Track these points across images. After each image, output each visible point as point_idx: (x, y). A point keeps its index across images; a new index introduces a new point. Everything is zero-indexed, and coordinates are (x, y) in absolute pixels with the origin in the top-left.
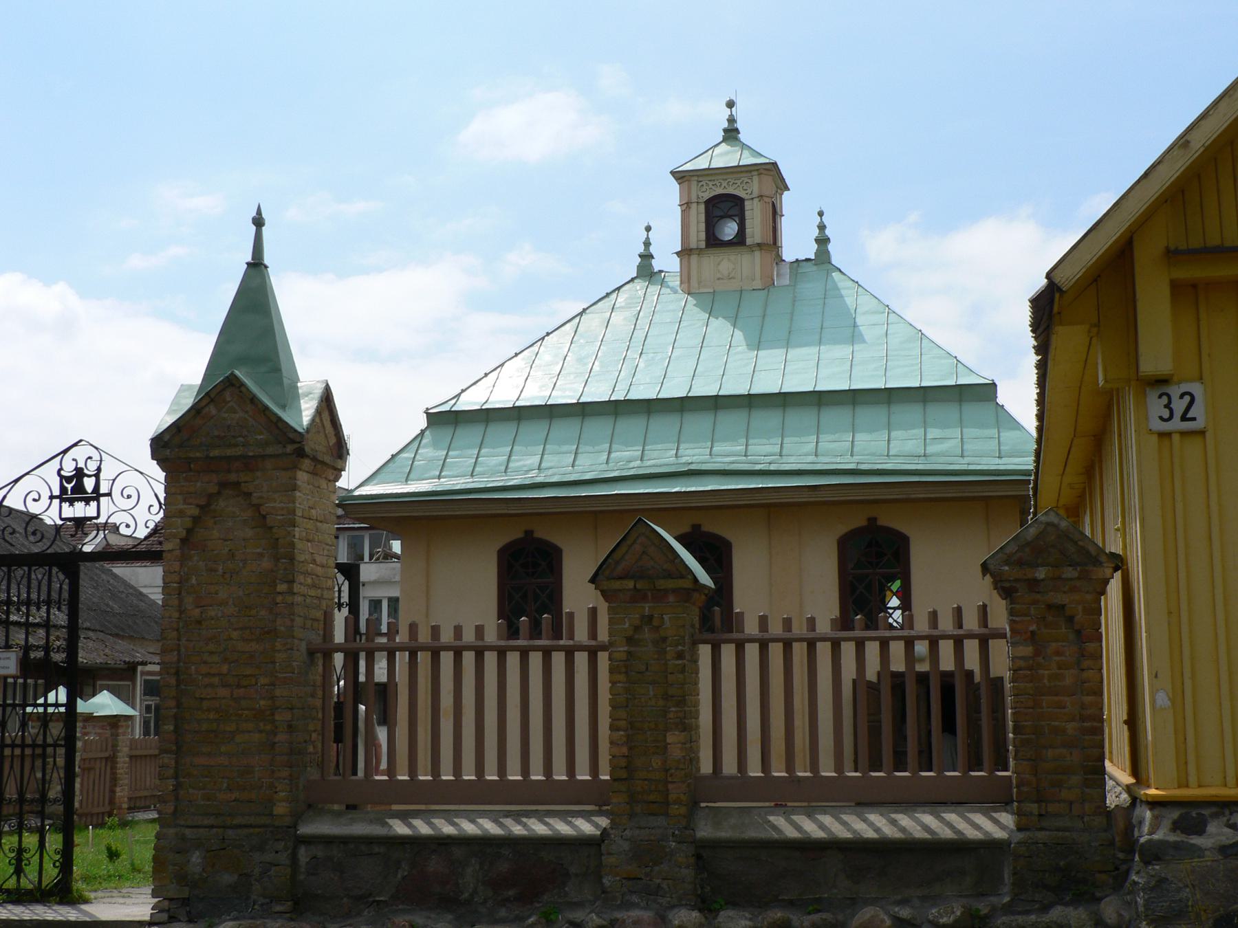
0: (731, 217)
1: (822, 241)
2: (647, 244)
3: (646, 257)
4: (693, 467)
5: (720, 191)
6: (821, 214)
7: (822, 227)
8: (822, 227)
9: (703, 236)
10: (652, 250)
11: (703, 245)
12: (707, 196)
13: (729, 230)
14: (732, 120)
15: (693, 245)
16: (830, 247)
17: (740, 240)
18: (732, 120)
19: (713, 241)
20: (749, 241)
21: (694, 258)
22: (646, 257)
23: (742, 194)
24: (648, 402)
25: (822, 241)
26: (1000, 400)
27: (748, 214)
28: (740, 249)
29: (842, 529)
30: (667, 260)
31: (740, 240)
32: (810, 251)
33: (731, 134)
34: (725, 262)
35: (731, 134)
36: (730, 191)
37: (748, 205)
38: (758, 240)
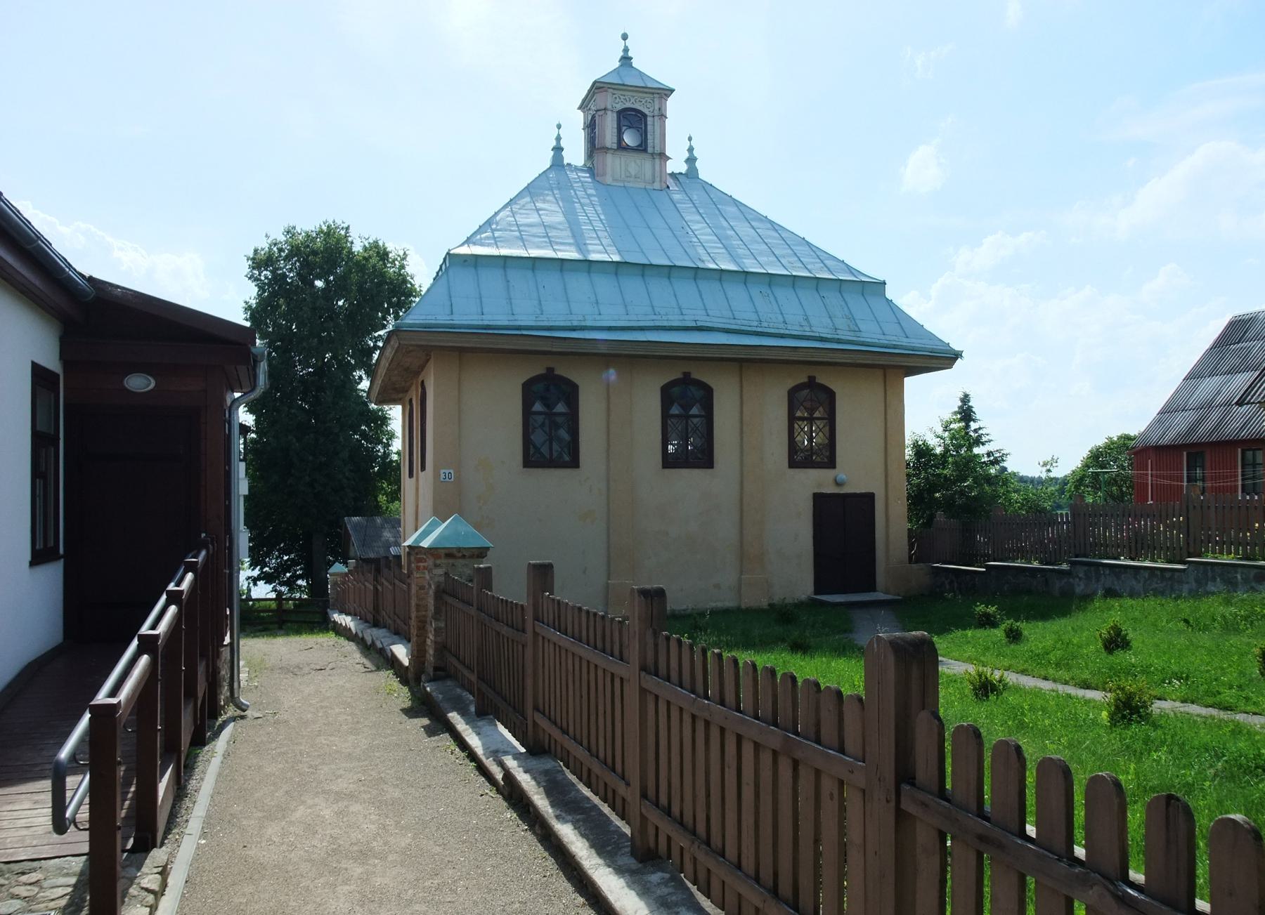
0: (638, 129)
1: (691, 160)
2: (558, 139)
3: (558, 149)
4: (699, 324)
5: (628, 105)
6: (690, 139)
7: (691, 150)
8: (691, 150)
9: (615, 140)
10: (563, 144)
11: (615, 146)
12: (619, 107)
13: (629, 139)
14: (626, 50)
15: (608, 144)
16: (697, 164)
17: (642, 148)
18: (626, 50)
19: (621, 147)
20: (650, 150)
21: (609, 158)
22: (558, 149)
23: (646, 111)
24: (644, 265)
25: (691, 160)
26: (889, 295)
27: (649, 128)
28: (643, 155)
29: (791, 383)
30: (575, 154)
31: (642, 148)
32: (683, 168)
33: (626, 60)
34: (634, 164)
35: (626, 60)
36: (637, 106)
37: (649, 119)
38: (657, 150)
